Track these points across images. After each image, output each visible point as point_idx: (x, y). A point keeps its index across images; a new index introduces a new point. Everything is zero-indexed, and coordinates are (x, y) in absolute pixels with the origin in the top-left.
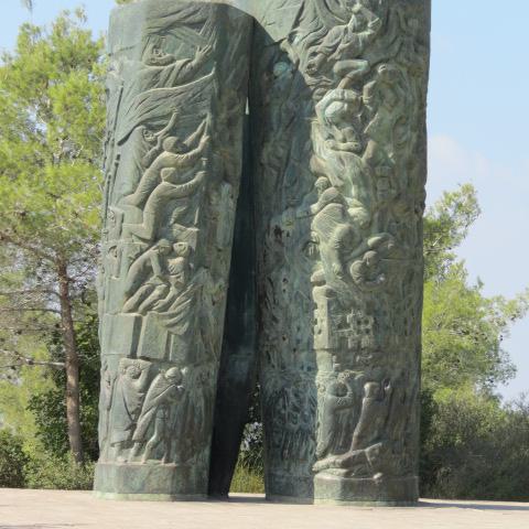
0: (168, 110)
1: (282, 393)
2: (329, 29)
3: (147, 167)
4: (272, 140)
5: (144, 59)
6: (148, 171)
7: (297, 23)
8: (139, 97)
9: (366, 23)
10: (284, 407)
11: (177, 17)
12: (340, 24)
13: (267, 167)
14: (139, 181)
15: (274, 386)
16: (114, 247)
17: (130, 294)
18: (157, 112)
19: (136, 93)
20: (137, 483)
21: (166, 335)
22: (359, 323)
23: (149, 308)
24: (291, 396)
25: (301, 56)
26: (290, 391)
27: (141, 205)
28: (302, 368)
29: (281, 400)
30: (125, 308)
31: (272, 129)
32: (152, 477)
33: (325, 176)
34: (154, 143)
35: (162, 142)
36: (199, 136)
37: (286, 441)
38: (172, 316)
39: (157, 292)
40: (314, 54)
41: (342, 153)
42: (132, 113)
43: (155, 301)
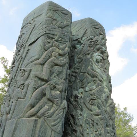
0: (56, 33)
2: (95, 37)
3: (46, 50)
5: (48, 15)
6: (46, 52)
7: (84, 35)
8: (45, 26)
11: (59, 9)
14: (42, 55)
16: (24, 84)
17: (33, 106)
18: (51, 32)
19: (43, 25)
21: (50, 131)
23: (43, 115)
25: (86, 43)
27: (43, 64)
30: (28, 114)
33: (96, 77)
34: (49, 43)
35: (53, 43)
36: (65, 47)
38: (55, 120)
39: (46, 107)
40: (91, 42)
42: (40, 31)
43: (46, 111)
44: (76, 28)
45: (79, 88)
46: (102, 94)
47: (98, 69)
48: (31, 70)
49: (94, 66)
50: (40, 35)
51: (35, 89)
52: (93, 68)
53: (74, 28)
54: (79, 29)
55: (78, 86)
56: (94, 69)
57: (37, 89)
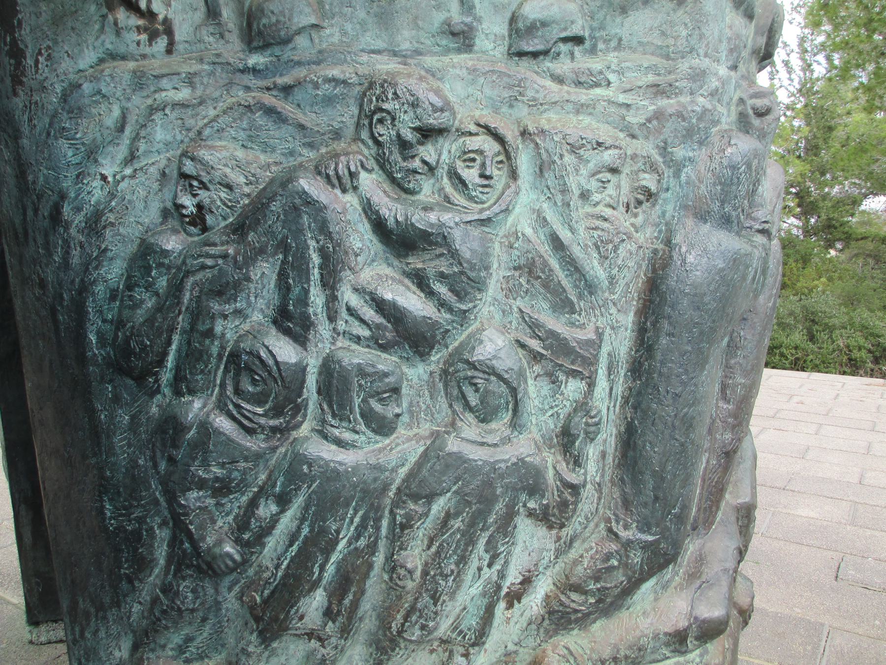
1: (276, 224)
10: (291, 321)
24: (360, 238)
37: (317, 544)
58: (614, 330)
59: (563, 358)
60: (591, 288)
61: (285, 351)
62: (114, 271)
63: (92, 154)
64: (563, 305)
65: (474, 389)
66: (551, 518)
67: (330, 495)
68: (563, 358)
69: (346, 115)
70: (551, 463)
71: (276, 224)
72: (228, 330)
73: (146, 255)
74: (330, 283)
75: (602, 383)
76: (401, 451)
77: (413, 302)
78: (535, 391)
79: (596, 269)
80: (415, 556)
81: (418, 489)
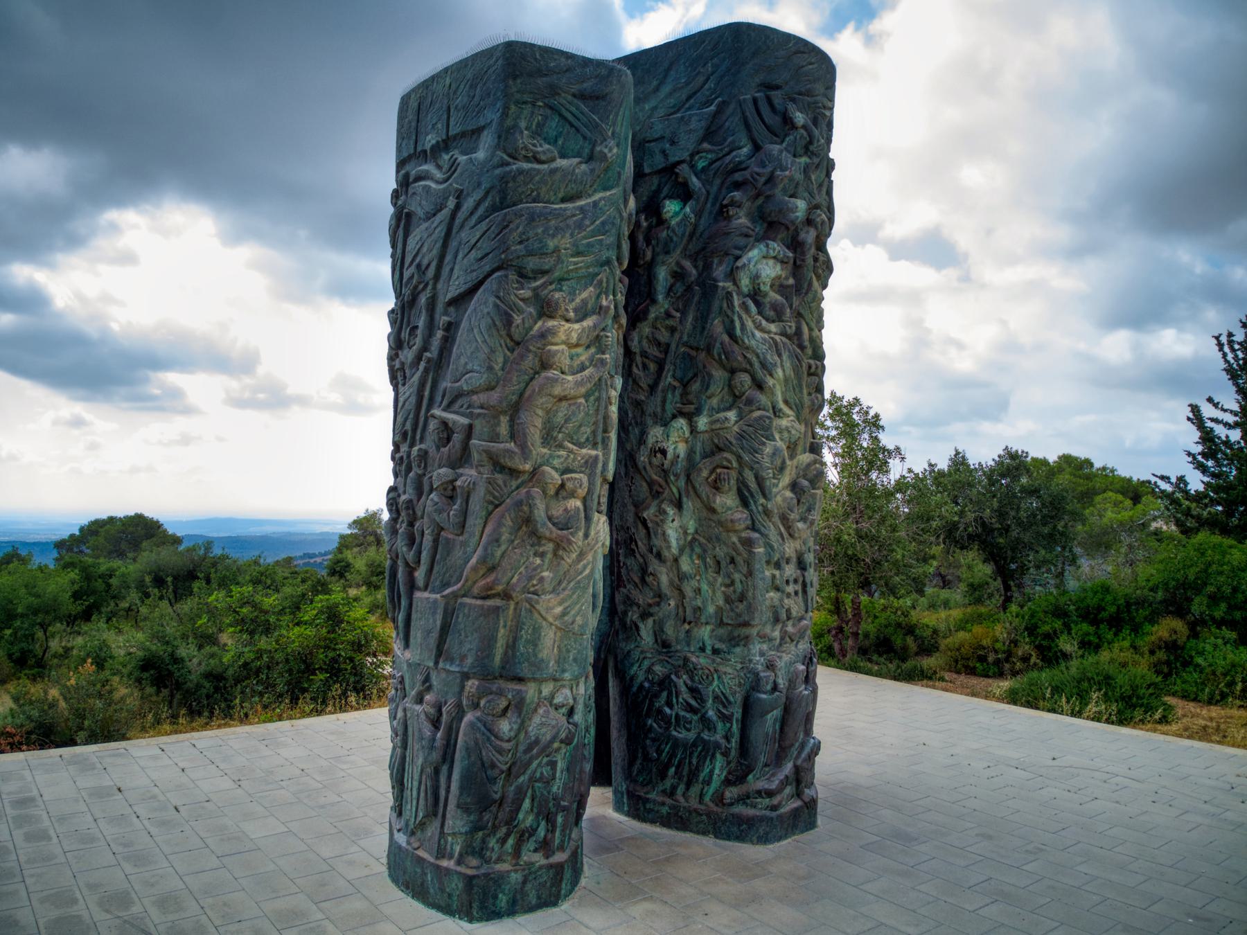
1: (665, 683)
4: (652, 315)
9: (811, 142)
10: (669, 704)
12: (776, 143)
13: (638, 359)
15: (649, 670)
20: (503, 900)
22: (787, 582)
24: (683, 689)
26: (681, 682)
28: (703, 649)
29: (665, 694)
31: (654, 302)
32: (529, 886)
37: (672, 755)
41: (777, 338)
44: (666, 89)
45: (674, 417)
46: (764, 444)
47: (759, 334)
48: (470, 427)
49: (740, 318)
50: (487, 268)
51: (491, 507)
52: (734, 328)
53: (657, 89)
54: (684, 97)
55: (670, 409)
56: (738, 332)
57: (497, 506)
58: (737, 712)
59: (726, 718)
60: (730, 703)
61: (668, 710)
62: (635, 689)
63: (632, 665)
64: (725, 707)
65: (706, 723)
66: (726, 754)
67: (676, 743)
68: (726, 718)
69: (681, 663)
70: (723, 742)
71: (665, 683)
72: (657, 705)
73: (641, 687)
74: (677, 697)
75: (735, 726)
76: (691, 736)
77: (693, 703)
78: (720, 725)
79: (731, 699)
80: (694, 761)
81: (694, 745)
